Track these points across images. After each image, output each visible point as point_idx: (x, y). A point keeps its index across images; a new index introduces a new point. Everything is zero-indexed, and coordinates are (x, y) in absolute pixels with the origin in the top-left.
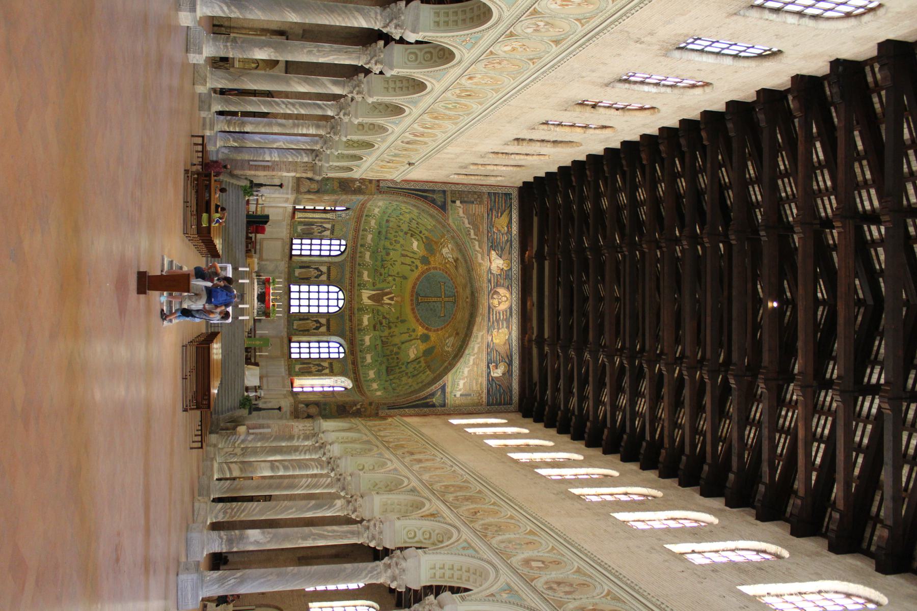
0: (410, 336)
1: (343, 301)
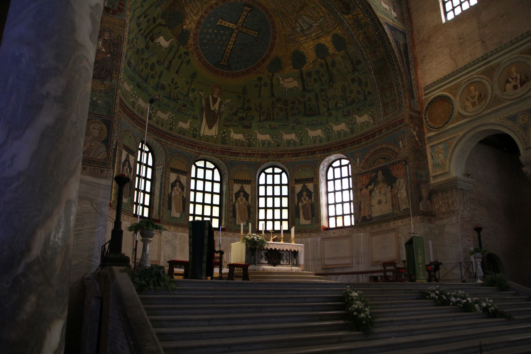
0: (266, 85)
1: (207, 162)
